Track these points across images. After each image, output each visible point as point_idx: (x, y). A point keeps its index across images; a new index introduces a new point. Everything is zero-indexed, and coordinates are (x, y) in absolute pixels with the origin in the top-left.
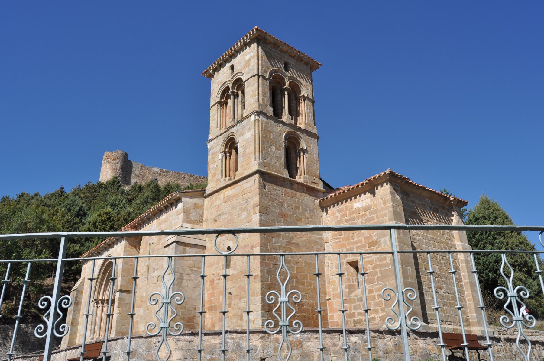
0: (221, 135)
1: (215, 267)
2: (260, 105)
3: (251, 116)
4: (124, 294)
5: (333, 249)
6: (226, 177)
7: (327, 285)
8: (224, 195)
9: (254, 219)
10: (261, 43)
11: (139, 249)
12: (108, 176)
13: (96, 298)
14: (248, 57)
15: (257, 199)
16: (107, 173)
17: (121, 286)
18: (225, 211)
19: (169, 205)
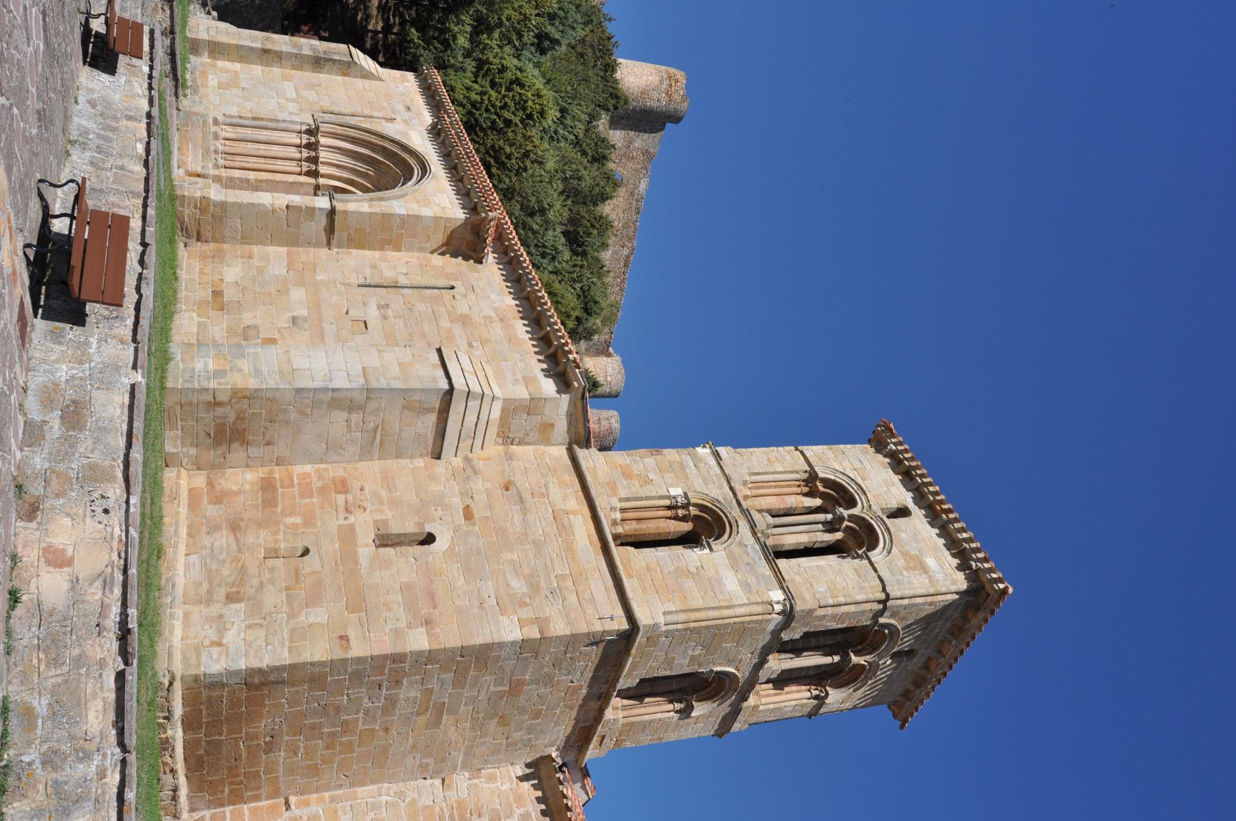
0: (731, 489)
1: (384, 493)
2: (811, 612)
3: (782, 588)
4: (324, 221)
5: (426, 807)
6: (623, 510)
7: (327, 795)
8: (575, 513)
9: (504, 620)
10: (968, 598)
11: (443, 254)
12: (631, 79)
13: (323, 128)
14: (931, 562)
15: (559, 628)
16: (637, 76)
17: (346, 212)
18: (531, 517)
19: (552, 350)
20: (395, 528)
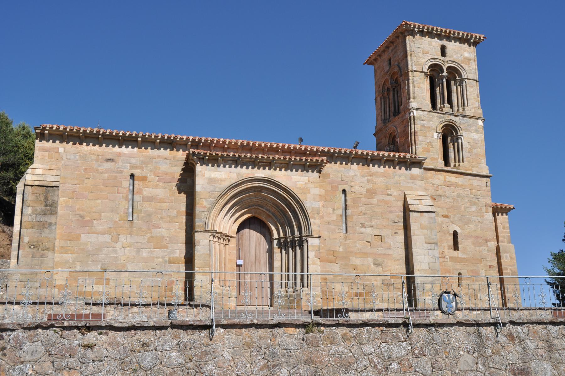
9: (486, 217)
18: (447, 195)
20: (451, 243)
